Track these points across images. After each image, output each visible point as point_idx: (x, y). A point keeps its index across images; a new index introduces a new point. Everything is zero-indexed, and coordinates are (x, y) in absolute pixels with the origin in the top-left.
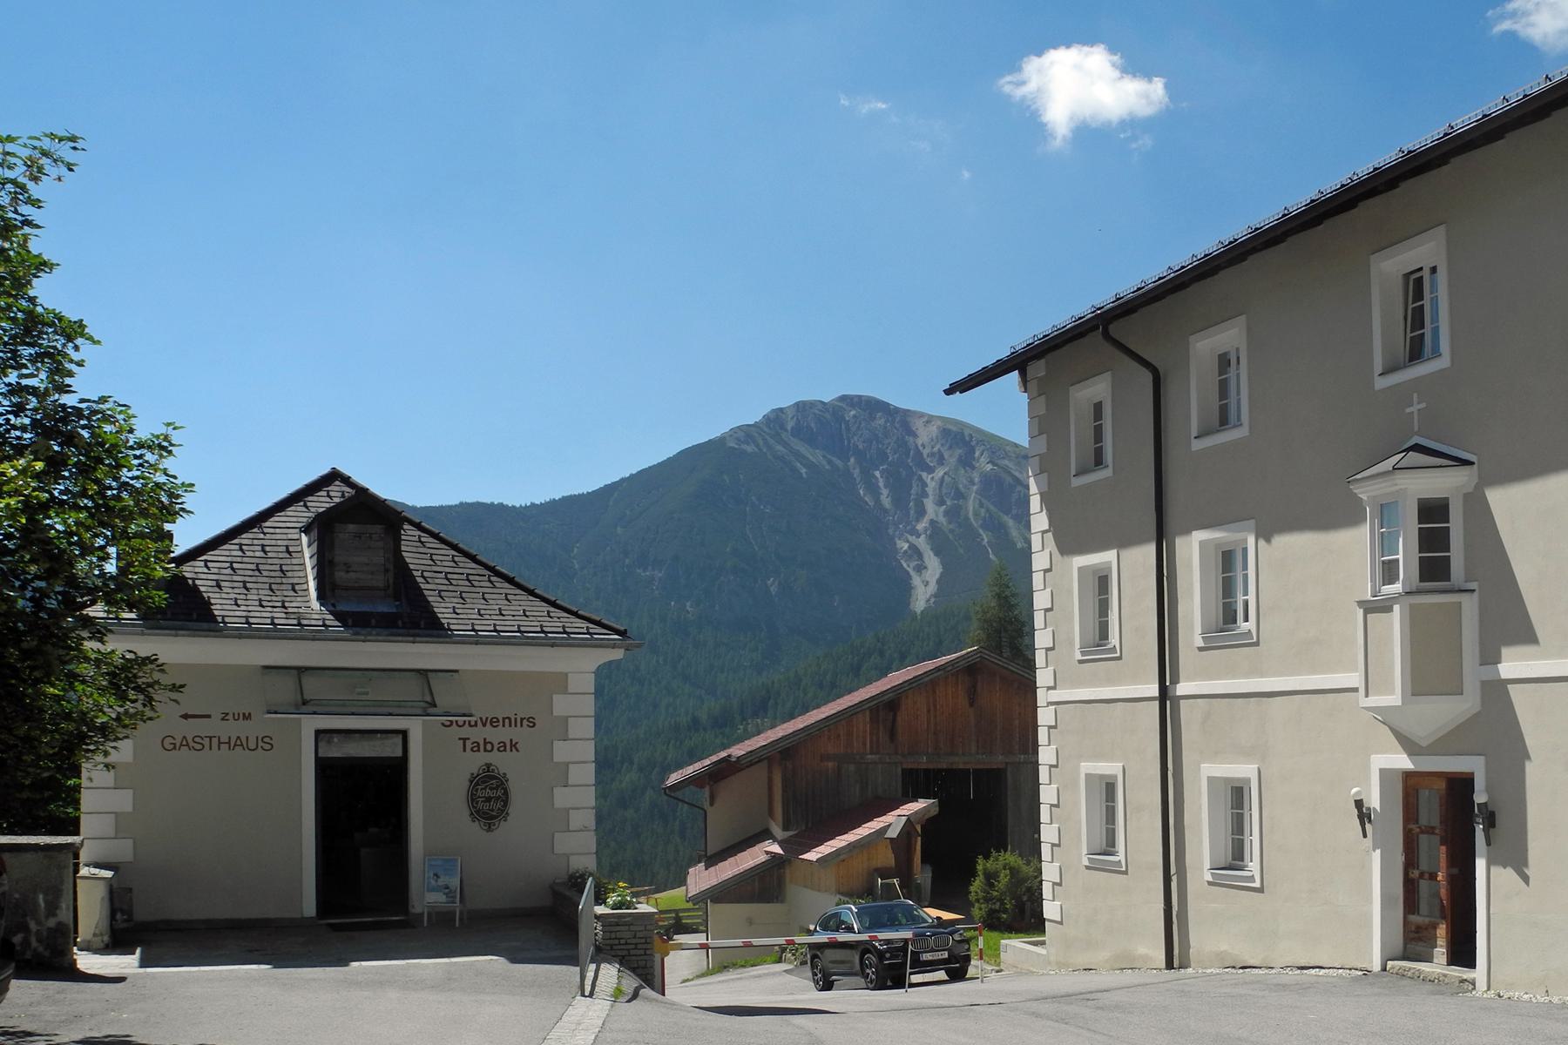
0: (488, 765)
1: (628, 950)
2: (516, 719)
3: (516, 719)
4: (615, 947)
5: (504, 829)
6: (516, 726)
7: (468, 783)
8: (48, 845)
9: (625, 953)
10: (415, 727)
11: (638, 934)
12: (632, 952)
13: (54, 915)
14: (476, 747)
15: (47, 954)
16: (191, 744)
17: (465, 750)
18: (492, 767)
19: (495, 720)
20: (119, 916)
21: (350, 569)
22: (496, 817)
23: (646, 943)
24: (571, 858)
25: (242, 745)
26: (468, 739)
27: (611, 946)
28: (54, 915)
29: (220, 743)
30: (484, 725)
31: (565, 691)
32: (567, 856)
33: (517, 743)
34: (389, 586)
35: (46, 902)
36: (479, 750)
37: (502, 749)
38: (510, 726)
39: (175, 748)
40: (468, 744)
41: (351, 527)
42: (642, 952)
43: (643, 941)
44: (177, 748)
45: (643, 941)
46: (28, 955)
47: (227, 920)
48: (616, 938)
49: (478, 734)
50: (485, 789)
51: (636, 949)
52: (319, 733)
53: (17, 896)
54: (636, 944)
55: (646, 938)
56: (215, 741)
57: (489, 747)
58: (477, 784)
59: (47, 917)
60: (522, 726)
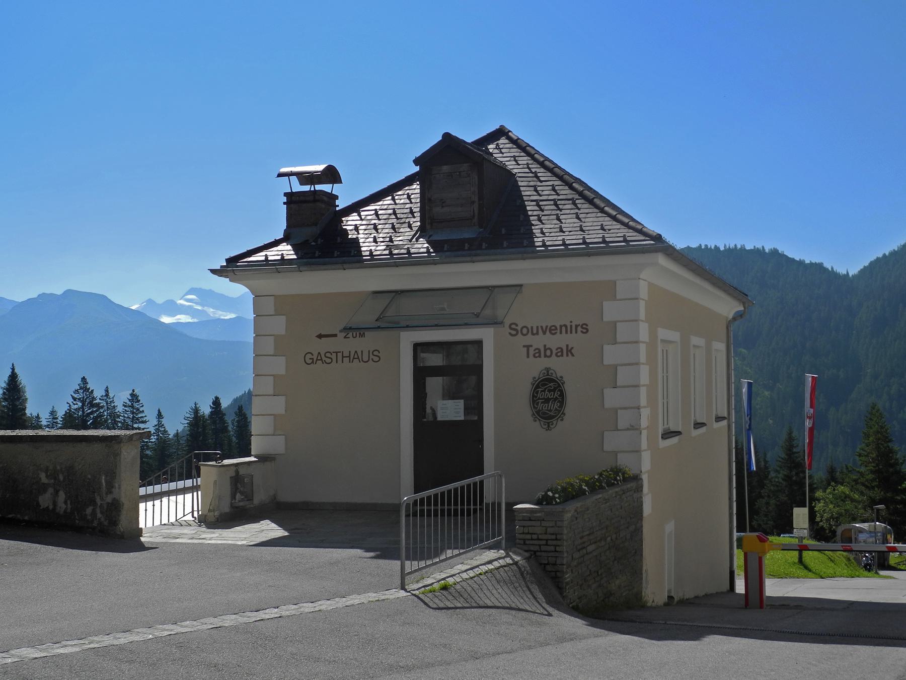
0: (548, 370)
1: (540, 545)
2: (571, 326)
3: (571, 326)
4: (527, 542)
5: (560, 426)
6: (571, 333)
7: (531, 386)
8: (103, 436)
9: (537, 548)
10: (486, 335)
11: (548, 529)
12: (543, 548)
13: (111, 492)
14: (538, 354)
15: (106, 523)
16: (324, 358)
17: (528, 357)
18: (552, 371)
19: (553, 328)
20: (238, 496)
21: (444, 205)
22: (553, 417)
23: (556, 539)
24: (619, 456)
25: (358, 358)
26: (531, 346)
27: (524, 540)
28: (111, 492)
29: (343, 357)
30: (544, 333)
31: (614, 297)
32: (615, 454)
33: (572, 348)
34: (474, 216)
35: (106, 481)
36: (540, 356)
37: (559, 354)
38: (566, 332)
39: (313, 362)
40: (532, 351)
41: (445, 168)
42: (552, 548)
43: (554, 537)
44: (314, 363)
45: (554, 537)
46: (95, 524)
47: (347, 503)
48: (528, 533)
49: (539, 341)
50: (544, 391)
51: (547, 545)
52: (418, 347)
53: (89, 476)
54: (547, 540)
55: (556, 535)
56: (340, 355)
57: (548, 353)
58: (538, 387)
59: (107, 494)
60: (576, 332)
